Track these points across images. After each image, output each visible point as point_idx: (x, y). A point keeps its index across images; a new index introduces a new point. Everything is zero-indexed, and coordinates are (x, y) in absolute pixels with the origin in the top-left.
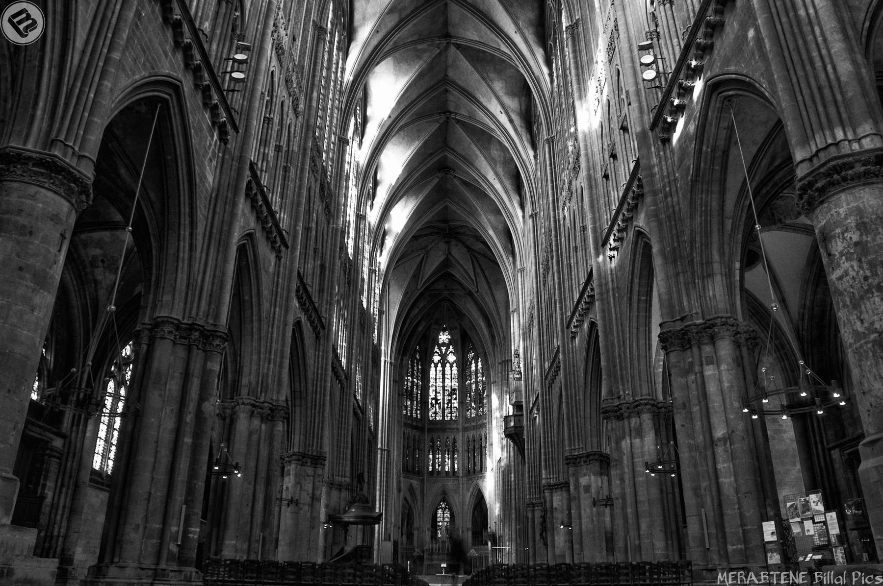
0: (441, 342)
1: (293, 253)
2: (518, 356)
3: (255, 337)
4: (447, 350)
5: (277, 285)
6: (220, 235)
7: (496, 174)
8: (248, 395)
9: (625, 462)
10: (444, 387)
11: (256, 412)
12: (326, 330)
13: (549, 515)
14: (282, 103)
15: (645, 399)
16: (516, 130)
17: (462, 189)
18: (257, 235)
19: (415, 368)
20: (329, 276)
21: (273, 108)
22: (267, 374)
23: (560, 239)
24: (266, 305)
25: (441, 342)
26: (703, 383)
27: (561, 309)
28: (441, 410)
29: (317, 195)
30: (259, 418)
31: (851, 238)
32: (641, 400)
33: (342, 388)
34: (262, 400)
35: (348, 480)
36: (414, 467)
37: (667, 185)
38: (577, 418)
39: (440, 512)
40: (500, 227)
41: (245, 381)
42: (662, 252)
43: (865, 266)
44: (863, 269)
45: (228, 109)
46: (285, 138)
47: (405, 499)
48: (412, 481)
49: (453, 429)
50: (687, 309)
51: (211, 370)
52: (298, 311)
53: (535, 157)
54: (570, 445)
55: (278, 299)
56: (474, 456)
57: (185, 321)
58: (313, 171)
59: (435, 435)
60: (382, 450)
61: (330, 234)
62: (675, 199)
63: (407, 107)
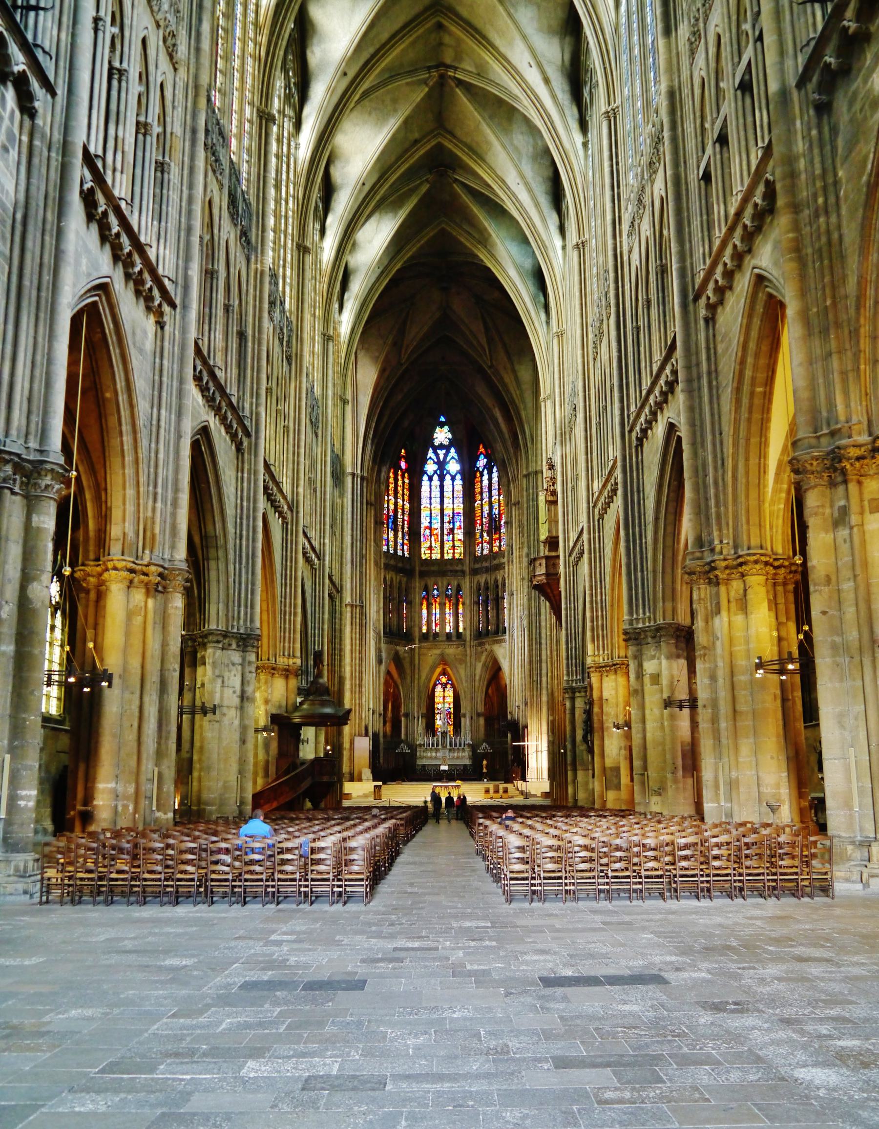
0: (437, 443)
1: (184, 317)
2: (551, 467)
3: (129, 458)
4: (446, 455)
5: (161, 371)
6: (39, 289)
7: (522, 176)
8: (123, 554)
9: (719, 650)
10: (442, 510)
11: (136, 580)
13: (596, 709)
14: (144, 41)
15: (754, 554)
16: (554, 97)
17: (466, 199)
18: (117, 286)
20: (253, 349)
21: (126, 49)
22: (153, 518)
23: (623, 286)
24: (143, 406)
25: (437, 443)
26: (863, 542)
27: (621, 400)
29: (225, 214)
30: (143, 590)
32: (749, 555)
33: (285, 523)
34: (146, 560)
35: (298, 661)
37: (820, 193)
38: (642, 571)
39: (439, 689)
40: (528, 264)
41: (115, 531)
42: (804, 316)
45: (28, 49)
46: (155, 109)
47: (388, 673)
49: (457, 571)
50: (842, 418)
51: (38, 528)
53: (585, 145)
54: (631, 613)
55: (164, 394)
56: (487, 611)
58: (214, 171)
59: (430, 581)
60: (352, 606)
62: (833, 219)
63: (373, 56)
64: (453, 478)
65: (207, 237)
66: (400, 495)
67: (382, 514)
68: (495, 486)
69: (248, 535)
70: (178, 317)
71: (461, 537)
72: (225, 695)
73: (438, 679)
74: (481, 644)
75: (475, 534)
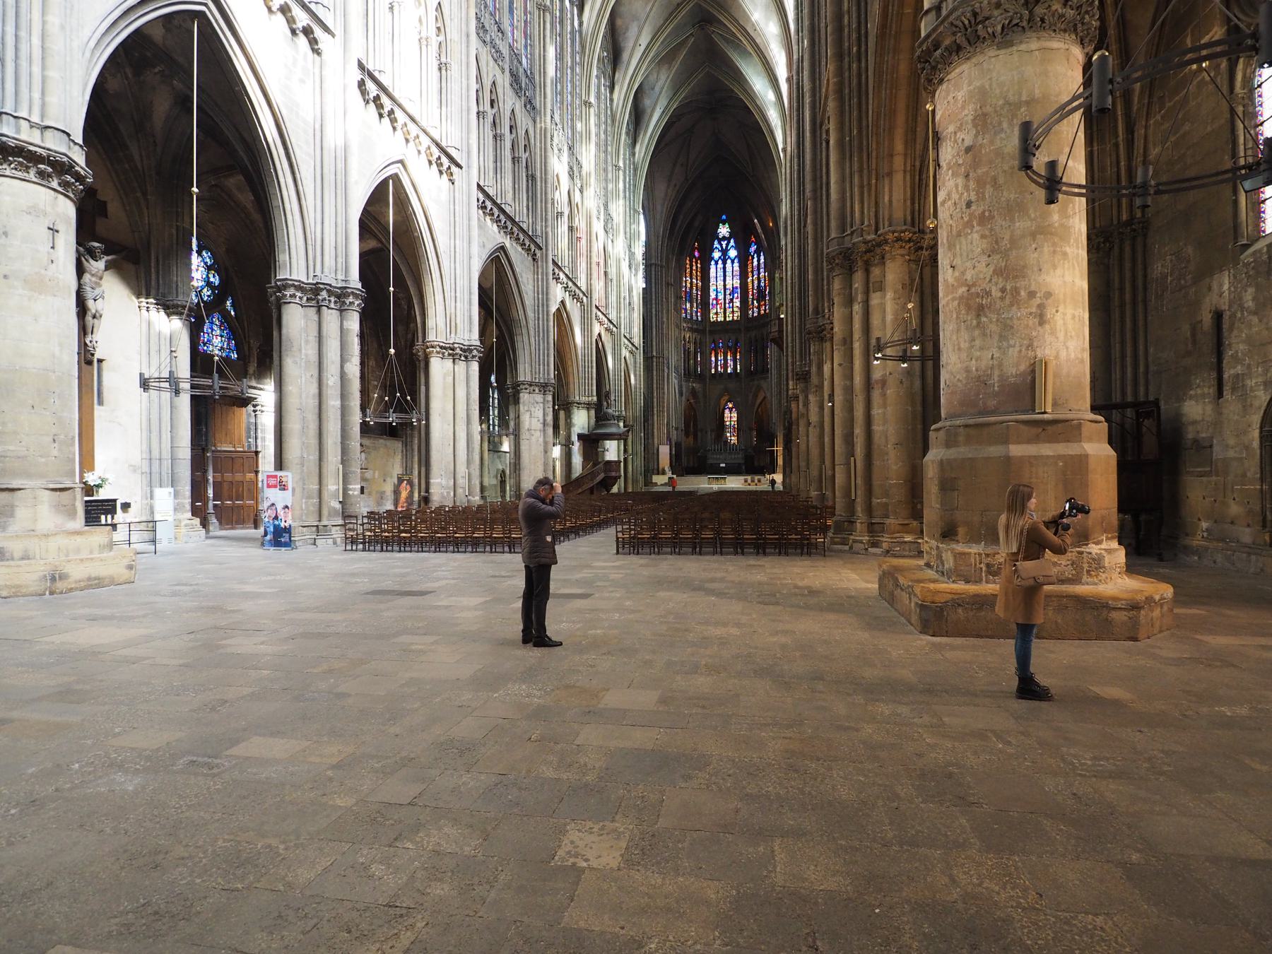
4: (727, 245)
12: (544, 250)
13: (794, 427)
19: (694, 268)
28: (722, 310)
31: (963, 140)
36: (696, 369)
39: (727, 411)
43: (972, 185)
44: (968, 190)
52: (498, 236)
57: (310, 281)
59: (717, 337)
61: (538, 136)
62: (863, 65)
64: (733, 262)
65: (490, 112)
68: (762, 266)
70: (464, 174)
72: (533, 422)
73: (726, 404)
74: (754, 380)
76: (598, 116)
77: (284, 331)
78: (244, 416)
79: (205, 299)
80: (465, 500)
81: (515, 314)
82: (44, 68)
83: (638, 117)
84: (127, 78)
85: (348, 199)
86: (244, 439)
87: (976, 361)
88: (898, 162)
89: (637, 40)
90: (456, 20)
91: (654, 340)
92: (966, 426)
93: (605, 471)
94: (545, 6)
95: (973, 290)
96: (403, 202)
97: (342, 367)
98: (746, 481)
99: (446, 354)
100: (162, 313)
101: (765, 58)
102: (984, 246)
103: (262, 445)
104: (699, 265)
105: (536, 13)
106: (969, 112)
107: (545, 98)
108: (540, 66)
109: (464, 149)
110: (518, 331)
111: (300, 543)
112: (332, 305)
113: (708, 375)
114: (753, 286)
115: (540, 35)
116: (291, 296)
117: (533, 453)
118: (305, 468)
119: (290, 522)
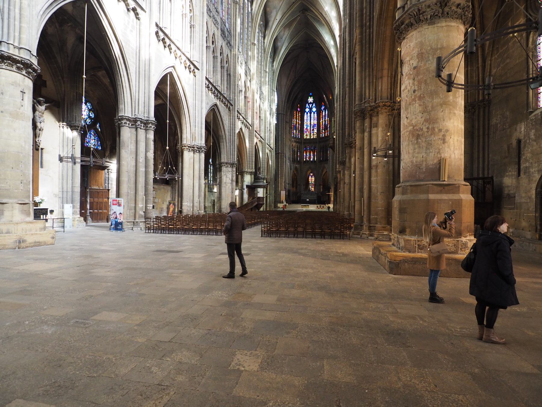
10: (310, 123)
13: (339, 184)
19: (298, 115)
31: (413, 64)
35: (254, 170)
39: (310, 177)
43: (416, 83)
48: (296, 165)
57: (133, 117)
61: (232, 57)
64: (314, 113)
65: (212, 47)
66: (298, 119)
67: (292, 125)
68: (327, 115)
69: (233, 135)
71: (316, 131)
73: (310, 174)
75: (320, 130)
76: (258, 49)
77: (121, 138)
78: (104, 174)
79: (88, 123)
80: (197, 212)
81: (220, 133)
82: (20, 22)
83: (275, 50)
84: (56, 28)
85: (150, 82)
86: (103, 184)
87: (416, 158)
88: (385, 72)
89: (276, 17)
90: (198, 7)
91: (280, 146)
92: (411, 186)
93: (258, 201)
94: (236, 2)
95: (415, 128)
96: (173, 84)
97: (146, 154)
98: (317, 207)
99: (191, 149)
100: (69, 129)
101: (330, 26)
102: (421, 109)
103: (111, 187)
104: (300, 114)
105: (233, 4)
106: (415, 52)
107: (235, 41)
108: (234, 27)
109: (200, 62)
110: (222, 141)
111: (126, 229)
112: (142, 128)
113: (302, 161)
114: (322, 124)
115: (234, 14)
116: (124, 123)
117: (227, 193)
118: (129, 197)
119: (122, 220)
